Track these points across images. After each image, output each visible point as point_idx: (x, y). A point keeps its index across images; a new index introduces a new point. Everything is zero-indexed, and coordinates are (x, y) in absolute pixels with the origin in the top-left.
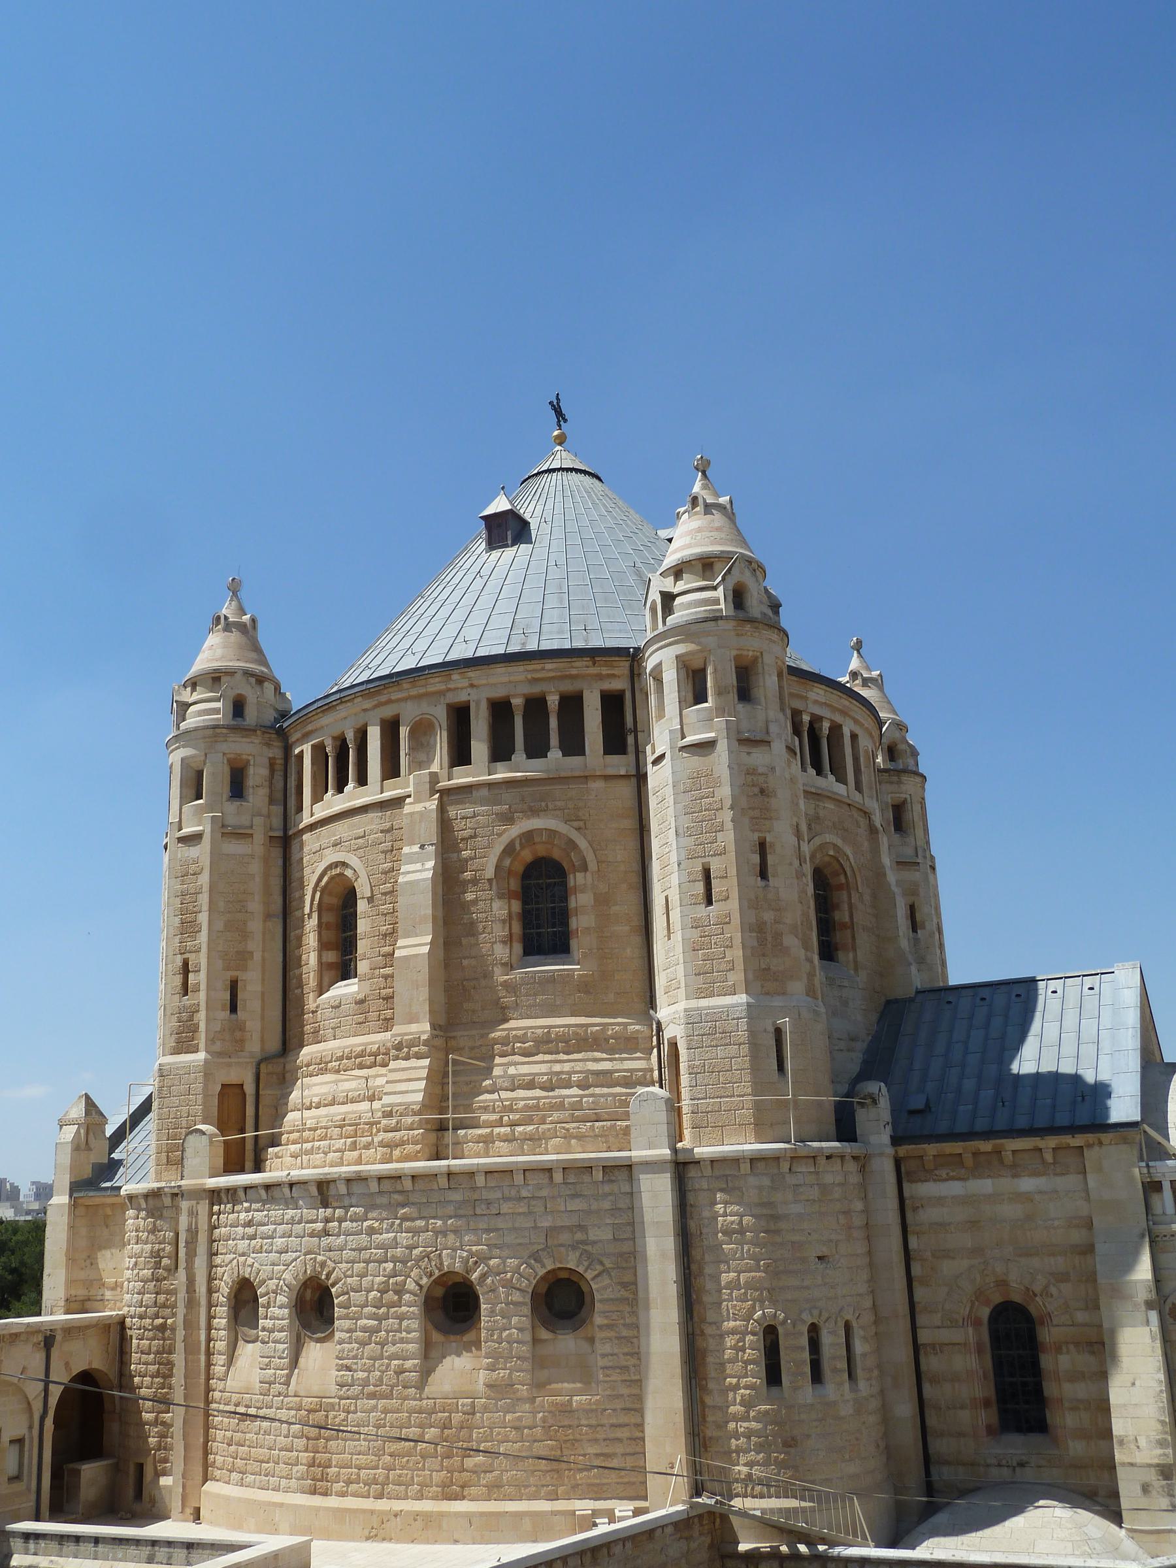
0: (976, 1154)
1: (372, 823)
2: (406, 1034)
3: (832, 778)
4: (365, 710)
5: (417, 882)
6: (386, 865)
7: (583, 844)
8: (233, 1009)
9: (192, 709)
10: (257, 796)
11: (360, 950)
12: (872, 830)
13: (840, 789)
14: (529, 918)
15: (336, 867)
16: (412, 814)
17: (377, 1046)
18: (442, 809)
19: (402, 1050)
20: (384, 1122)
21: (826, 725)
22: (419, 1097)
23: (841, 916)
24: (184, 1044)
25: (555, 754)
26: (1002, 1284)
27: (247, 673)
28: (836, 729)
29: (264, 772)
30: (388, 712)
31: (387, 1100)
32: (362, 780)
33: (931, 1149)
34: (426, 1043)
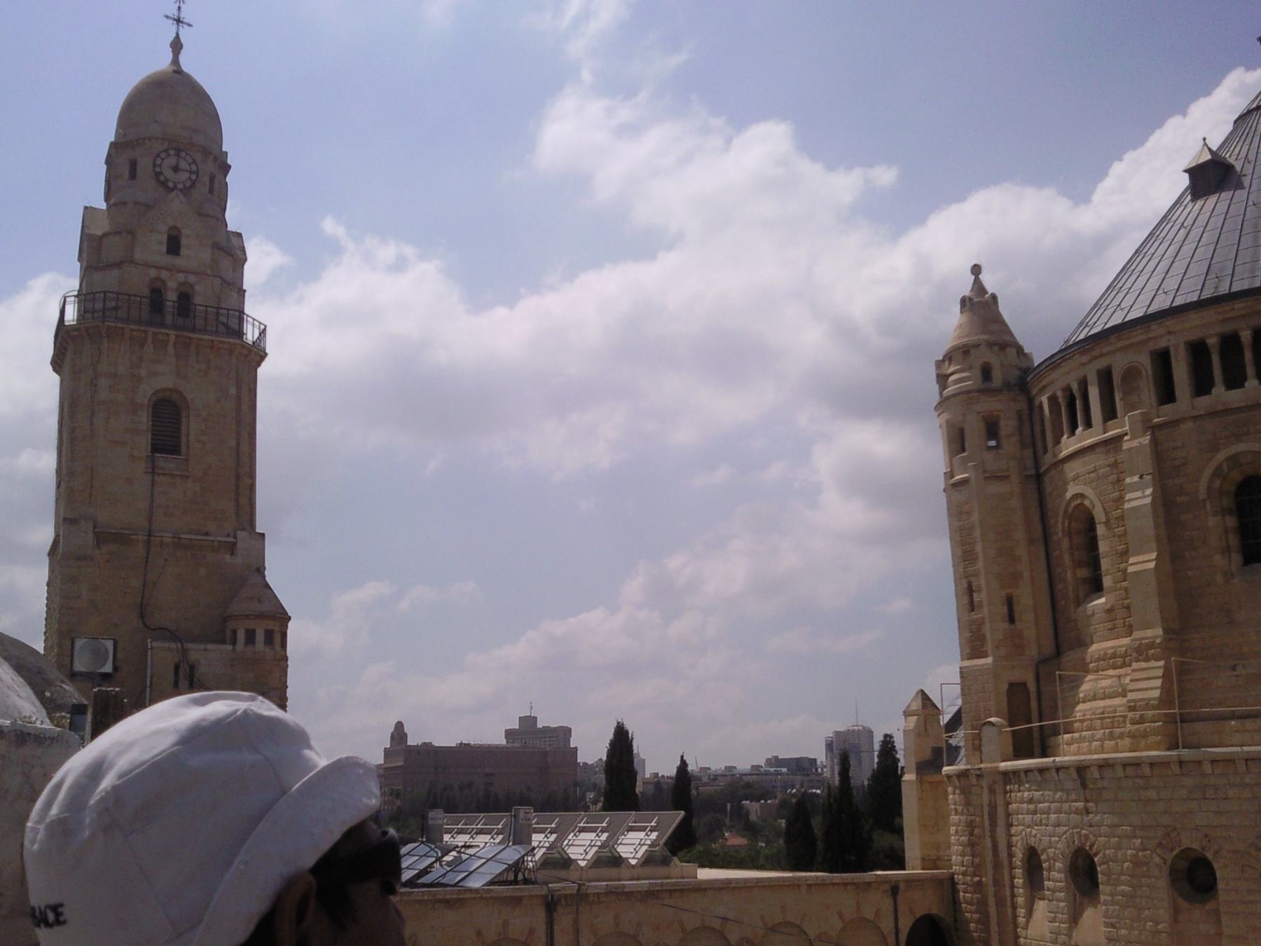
1: (1098, 460)
2: (1143, 639)
4: (1083, 364)
5: (1140, 506)
6: (1115, 494)
9: (952, 378)
10: (1010, 445)
11: (1103, 568)
15: (1077, 498)
16: (1130, 449)
17: (1124, 649)
19: (1141, 652)
20: (1130, 715)
22: (1156, 693)
27: (990, 345)
30: (1102, 363)
31: (1131, 696)
32: (1088, 424)
34: (1159, 646)
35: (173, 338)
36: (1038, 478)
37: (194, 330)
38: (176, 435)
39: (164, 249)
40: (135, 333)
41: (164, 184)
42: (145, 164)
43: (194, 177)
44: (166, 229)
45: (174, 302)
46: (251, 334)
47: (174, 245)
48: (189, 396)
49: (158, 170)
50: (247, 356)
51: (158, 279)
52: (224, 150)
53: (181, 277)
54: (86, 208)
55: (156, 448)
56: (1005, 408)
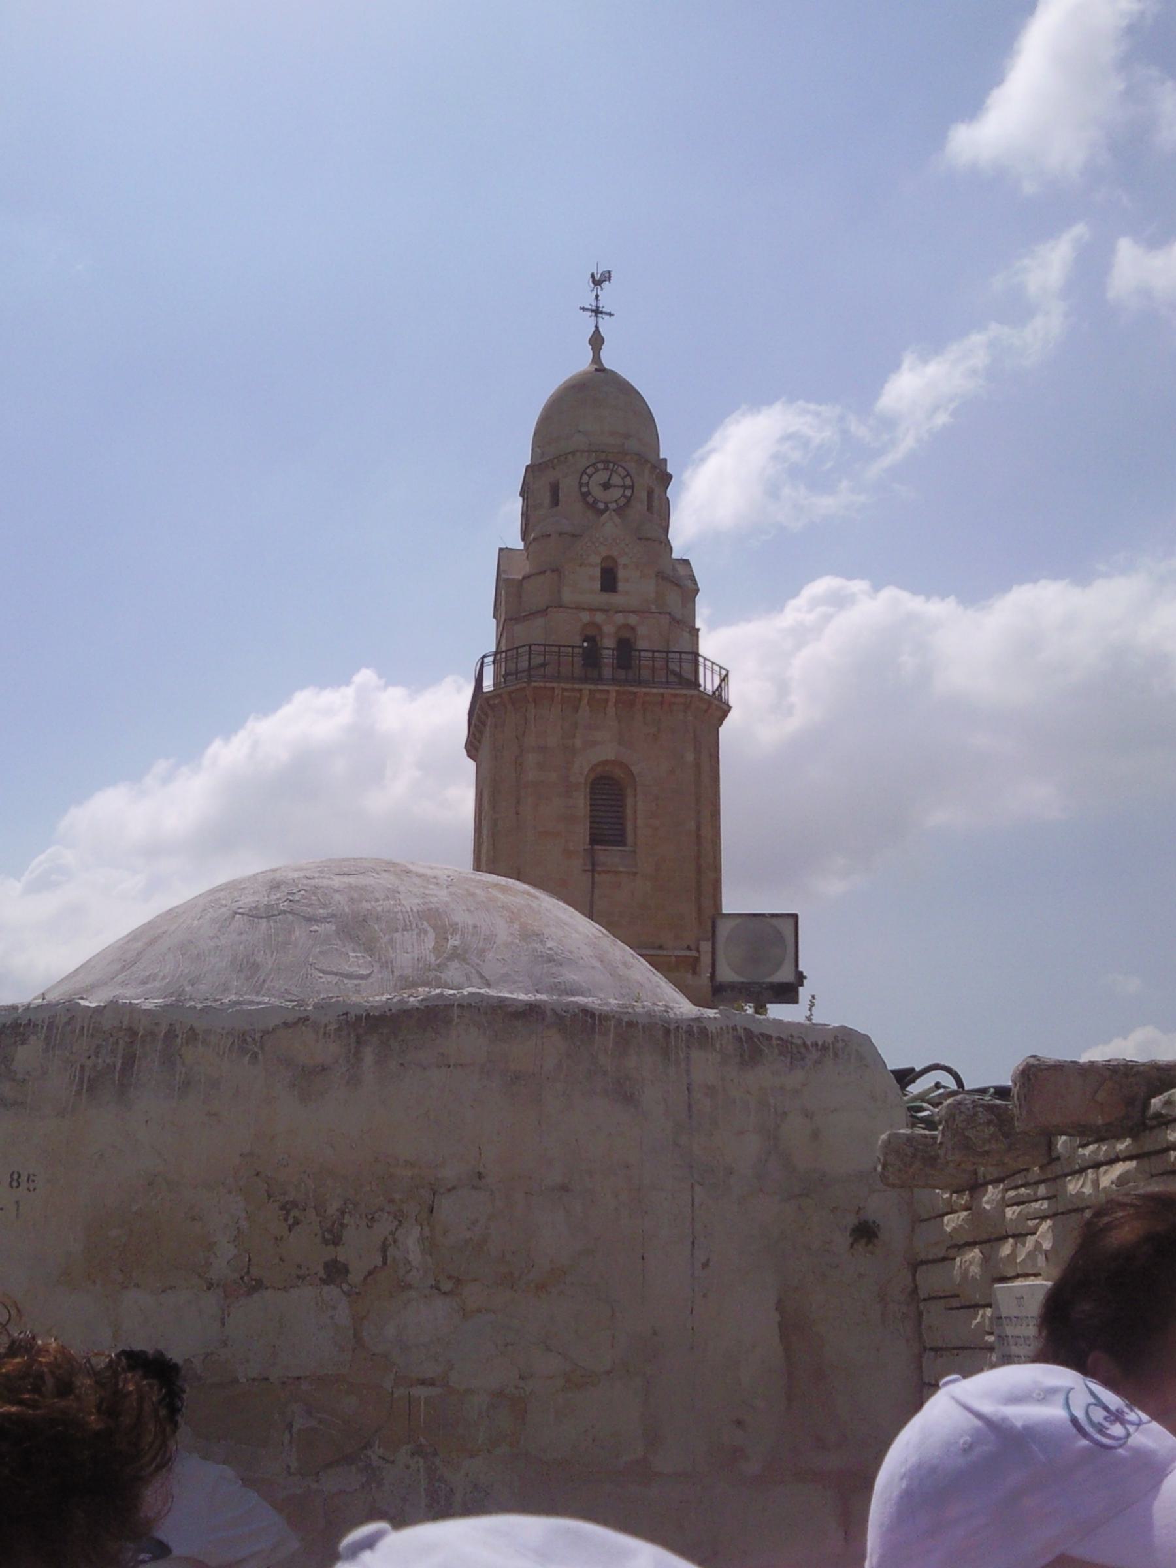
35: (613, 696)
37: (640, 683)
38: (619, 827)
39: (598, 585)
40: (566, 694)
41: (593, 506)
42: (569, 485)
43: (628, 493)
44: (599, 561)
45: (613, 650)
46: (708, 682)
47: (609, 581)
48: (635, 770)
49: (584, 489)
50: (706, 711)
51: (592, 624)
52: (662, 457)
53: (619, 619)
54: (501, 550)
55: (596, 839)
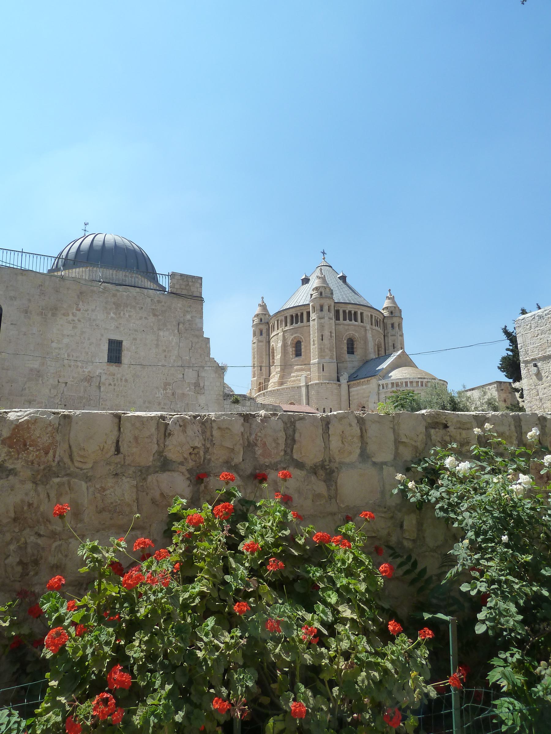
0: (358, 383)
3: (353, 321)
7: (303, 338)
8: (261, 370)
12: (366, 330)
13: (356, 323)
14: (296, 351)
18: (283, 334)
21: (353, 312)
23: (355, 346)
24: (254, 377)
25: (299, 323)
26: (361, 403)
27: (262, 314)
28: (355, 313)
29: (266, 331)
30: (277, 319)
33: (352, 383)
36: (269, 342)
56: (264, 328)
